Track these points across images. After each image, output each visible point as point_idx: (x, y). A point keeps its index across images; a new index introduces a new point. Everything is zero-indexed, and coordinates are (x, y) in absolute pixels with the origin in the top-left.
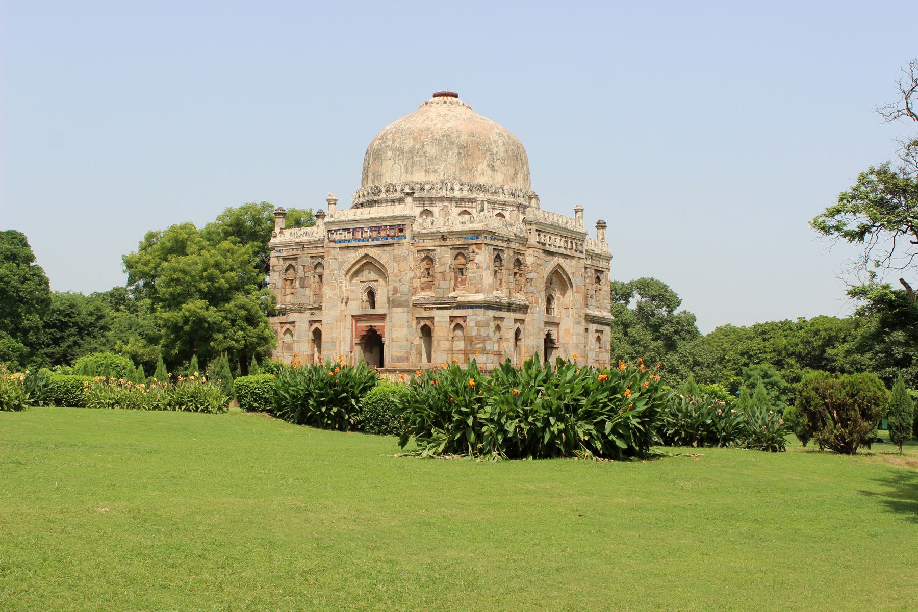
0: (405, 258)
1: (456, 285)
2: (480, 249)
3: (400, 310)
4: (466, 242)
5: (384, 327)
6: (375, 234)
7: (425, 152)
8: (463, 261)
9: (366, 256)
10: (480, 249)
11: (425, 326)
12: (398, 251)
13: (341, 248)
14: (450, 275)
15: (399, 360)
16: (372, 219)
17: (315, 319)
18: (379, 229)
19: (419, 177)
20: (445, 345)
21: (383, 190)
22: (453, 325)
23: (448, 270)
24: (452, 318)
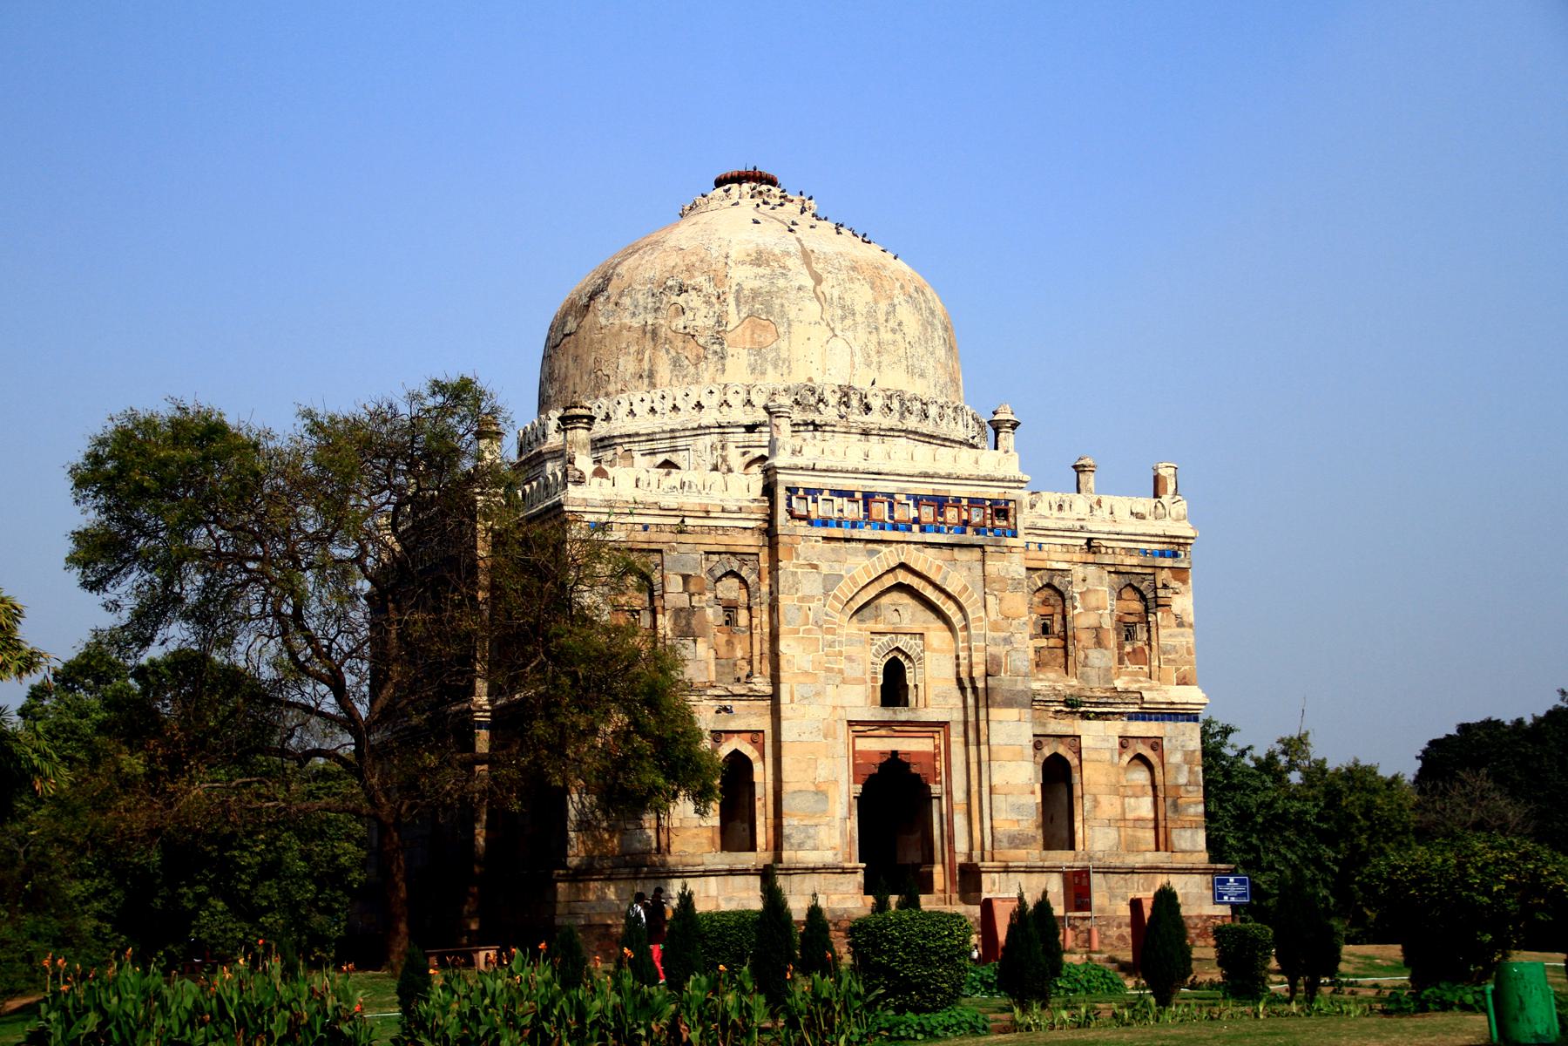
0: (1017, 585)
1: (1121, 661)
2: (1184, 582)
3: (1012, 713)
4: (1149, 561)
5: (935, 756)
6: (927, 513)
7: (900, 324)
8: (1137, 606)
9: (903, 566)
10: (1184, 582)
11: (1056, 756)
12: (994, 566)
13: (827, 539)
14: (1112, 639)
15: (1017, 841)
16: (926, 475)
17: (732, 726)
18: (940, 503)
19: (894, 379)
20: (1109, 806)
21: (833, 400)
22: (1126, 758)
23: (1108, 623)
24: (1125, 741)
